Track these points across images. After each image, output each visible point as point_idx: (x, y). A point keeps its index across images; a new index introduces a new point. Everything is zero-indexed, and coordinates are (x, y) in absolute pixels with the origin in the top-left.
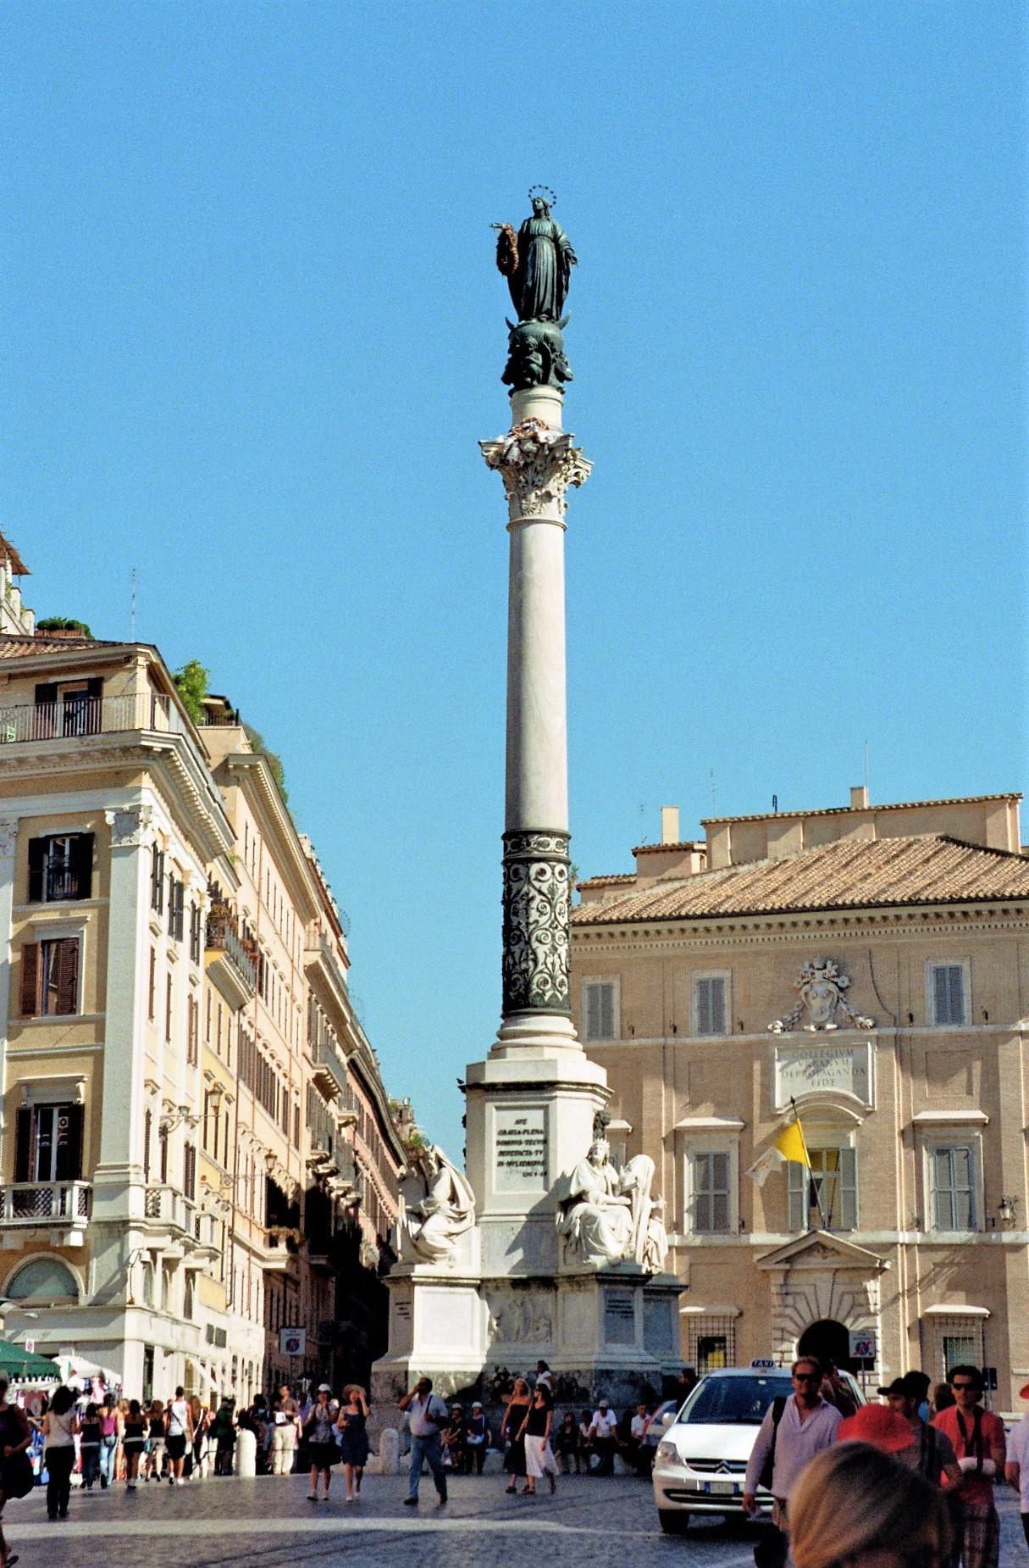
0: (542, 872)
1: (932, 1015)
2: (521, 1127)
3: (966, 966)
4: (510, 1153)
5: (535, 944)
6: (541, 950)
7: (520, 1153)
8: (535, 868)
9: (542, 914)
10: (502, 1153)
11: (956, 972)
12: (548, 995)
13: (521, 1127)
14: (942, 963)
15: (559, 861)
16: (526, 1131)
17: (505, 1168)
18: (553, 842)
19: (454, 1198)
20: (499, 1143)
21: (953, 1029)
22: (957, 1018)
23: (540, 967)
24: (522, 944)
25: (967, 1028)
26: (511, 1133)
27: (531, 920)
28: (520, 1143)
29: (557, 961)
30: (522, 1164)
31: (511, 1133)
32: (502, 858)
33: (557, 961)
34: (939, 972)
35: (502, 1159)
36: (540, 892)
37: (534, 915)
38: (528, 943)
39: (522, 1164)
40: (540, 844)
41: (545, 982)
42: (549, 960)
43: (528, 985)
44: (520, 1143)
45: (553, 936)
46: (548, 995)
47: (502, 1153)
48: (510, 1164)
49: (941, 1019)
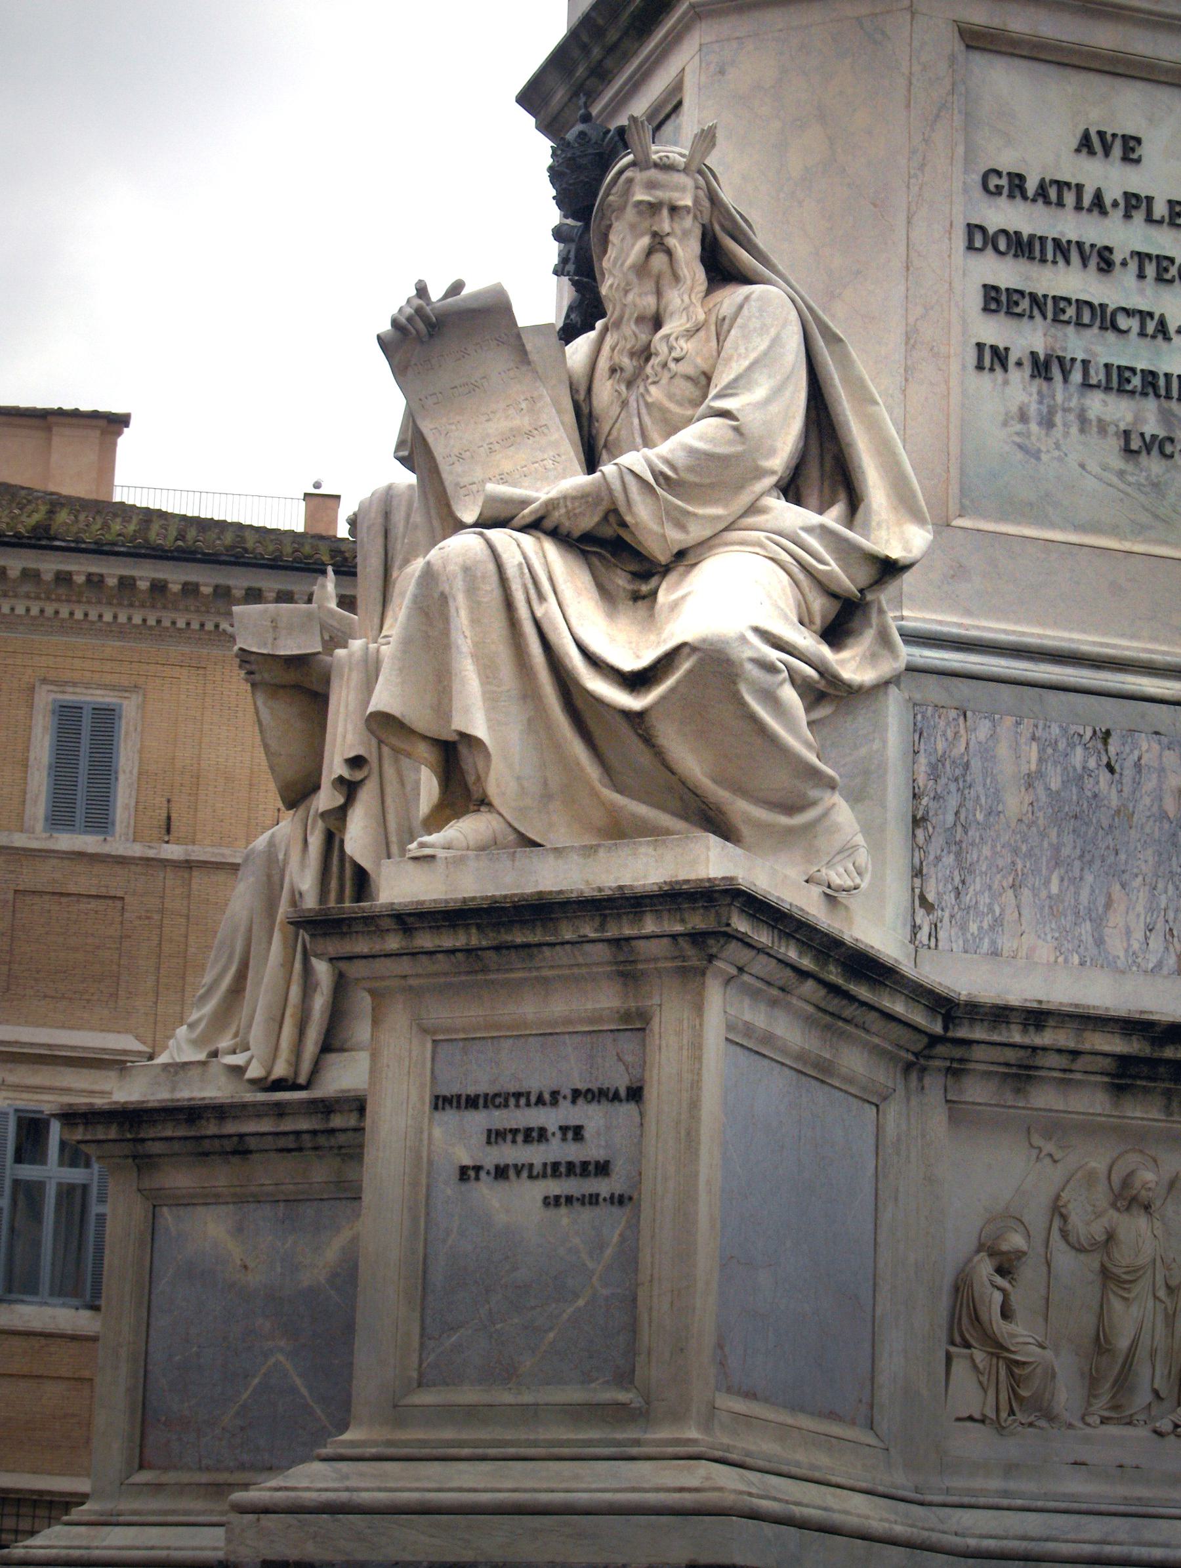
1: (38, 808)
2: (1111, 177)
3: (130, 708)
4: (1053, 309)
7: (1106, 319)
10: (996, 300)
11: (107, 717)
13: (1111, 177)
14: (70, 696)
16: (1133, 203)
17: (1019, 388)
19: (824, 466)
20: (979, 238)
21: (89, 843)
22: (100, 821)
25: (118, 845)
26: (1051, 193)
28: (1105, 260)
30: (1119, 381)
31: (1051, 193)
34: (68, 718)
35: (994, 331)
39: (1119, 381)
44: (1105, 260)
47: (996, 300)
48: (1041, 367)
49: (60, 817)
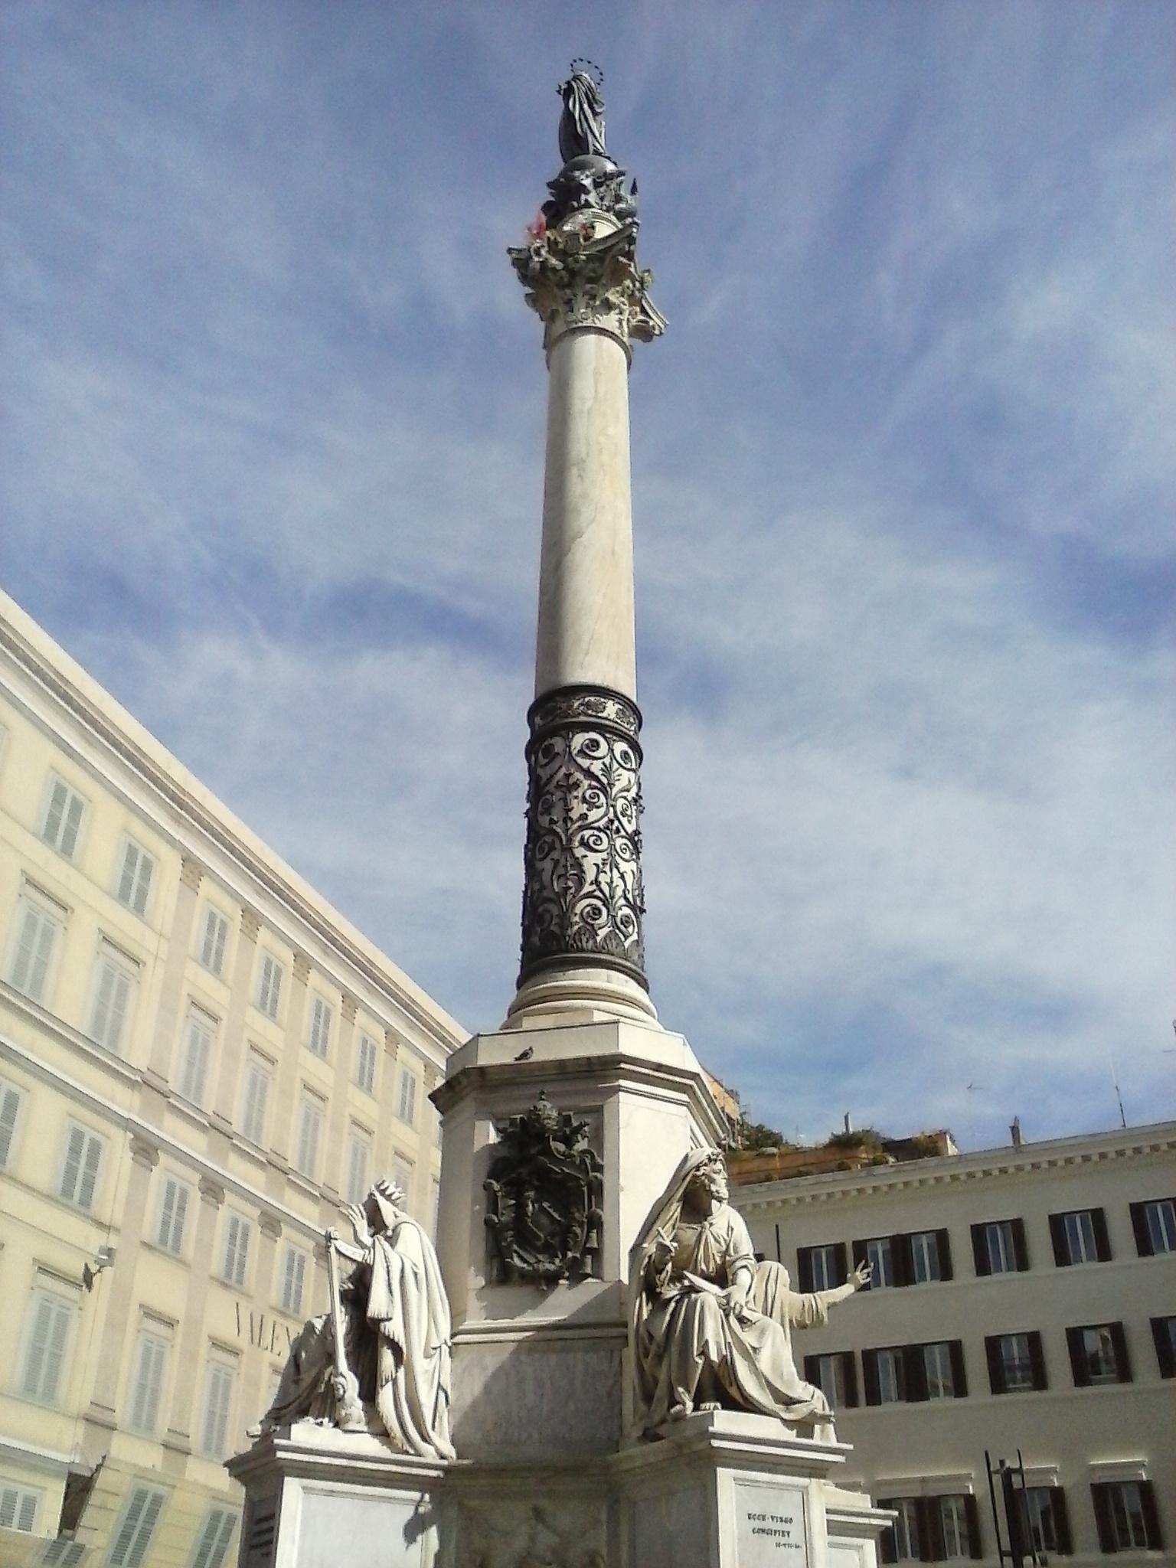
0: (595, 744)
5: (580, 852)
6: (591, 861)
8: (579, 740)
9: (592, 806)
12: (602, 933)
15: (623, 737)
18: (611, 709)
23: (587, 888)
24: (556, 855)
27: (574, 815)
29: (617, 881)
32: (526, 734)
33: (617, 881)
36: (589, 774)
37: (578, 808)
38: (568, 849)
40: (588, 705)
41: (597, 912)
42: (603, 878)
43: (565, 919)
45: (612, 846)
46: (602, 933)
